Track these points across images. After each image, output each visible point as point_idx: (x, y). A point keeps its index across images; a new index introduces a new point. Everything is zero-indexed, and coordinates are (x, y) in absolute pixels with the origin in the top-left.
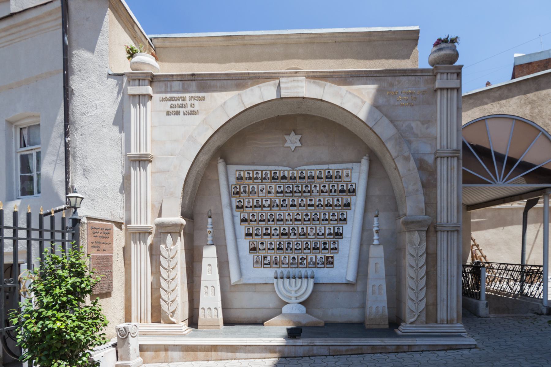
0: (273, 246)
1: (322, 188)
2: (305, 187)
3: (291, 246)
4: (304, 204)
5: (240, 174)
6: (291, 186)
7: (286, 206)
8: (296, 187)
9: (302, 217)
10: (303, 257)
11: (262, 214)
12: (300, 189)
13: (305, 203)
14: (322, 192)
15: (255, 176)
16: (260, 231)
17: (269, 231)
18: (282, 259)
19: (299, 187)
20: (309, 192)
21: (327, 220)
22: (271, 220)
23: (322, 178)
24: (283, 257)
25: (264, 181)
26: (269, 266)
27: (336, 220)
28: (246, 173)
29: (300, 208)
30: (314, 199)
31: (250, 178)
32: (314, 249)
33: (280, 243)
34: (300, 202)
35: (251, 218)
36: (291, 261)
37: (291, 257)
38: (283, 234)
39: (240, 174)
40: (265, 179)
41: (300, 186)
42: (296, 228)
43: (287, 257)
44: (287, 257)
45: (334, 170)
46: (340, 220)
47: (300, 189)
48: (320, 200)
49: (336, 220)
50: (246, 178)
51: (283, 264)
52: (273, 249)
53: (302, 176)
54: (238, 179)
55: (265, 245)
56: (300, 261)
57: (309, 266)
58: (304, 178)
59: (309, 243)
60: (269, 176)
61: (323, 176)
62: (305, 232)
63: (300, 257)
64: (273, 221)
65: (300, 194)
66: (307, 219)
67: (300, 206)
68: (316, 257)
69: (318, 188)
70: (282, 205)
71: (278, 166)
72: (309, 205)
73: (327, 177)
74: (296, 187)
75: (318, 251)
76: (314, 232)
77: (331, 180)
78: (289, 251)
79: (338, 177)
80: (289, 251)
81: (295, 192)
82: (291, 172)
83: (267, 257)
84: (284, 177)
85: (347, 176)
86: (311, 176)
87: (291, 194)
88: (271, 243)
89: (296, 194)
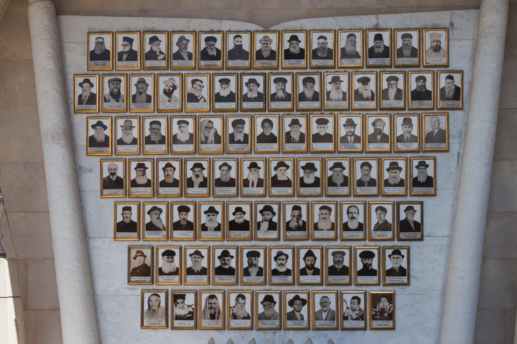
0: (204, 263)
1: (357, 86)
2: (305, 81)
3: (261, 262)
4: (302, 135)
5: (100, 43)
6: (260, 79)
7: (246, 141)
8: (276, 81)
9: (295, 172)
10: (297, 298)
11: (169, 165)
12: (289, 90)
13: (303, 130)
14: (359, 96)
15: (147, 48)
16: (163, 216)
17: (190, 217)
18: (233, 303)
19: (285, 81)
20: (316, 97)
21: (372, 183)
22: (197, 181)
23: (357, 56)
24: (233, 297)
25: (175, 63)
26: (192, 323)
27: (401, 183)
28: (120, 38)
29: (289, 147)
30: (331, 119)
31: (132, 56)
32: (332, 271)
33: (225, 254)
34: (287, 129)
35: (134, 175)
36: (261, 309)
37: (261, 297)
38: (234, 226)
39: (100, 43)
40: (178, 56)
41: (289, 78)
42: (275, 208)
43: (248, 296)
44: (248, 296)
45: (393, 32)
46: (416, 183)
47: (289, 90)
48: (350, 123)
49: (401, 183)
50: (121, 54)
51: (235, 317)
52: (204, 271)
53: (295, 50)
54: (93, 56)
55: (177, 258)
56: (289, 309)
57: (318, 323)
58: (301, 55)
59: (317, 253)
60: (191, 48)
61: (359, 48)
62: (304, 218)
63: (290, 297)
64: (203, 184)
65: (288, 105)
66: (309, 180)
67: (289, 139)
68: (339, 297)
69: (344, 87)
70: (232, 136)
71: (221, 18)
72: (317, 138)
73: (372, 53)
74: (276, 81)
75: (346, 279)
76: (332, 219)
77: (387, 61)
79: (407, 52)
80: (253, 278)
81: (274, 98)
82: (259, 37)
83: (183, 297)
84: (238, 53)
85: (437, 49)
86: (323, 48)
87: (261, 105)
88: (197, 253)
89: (274, 105)
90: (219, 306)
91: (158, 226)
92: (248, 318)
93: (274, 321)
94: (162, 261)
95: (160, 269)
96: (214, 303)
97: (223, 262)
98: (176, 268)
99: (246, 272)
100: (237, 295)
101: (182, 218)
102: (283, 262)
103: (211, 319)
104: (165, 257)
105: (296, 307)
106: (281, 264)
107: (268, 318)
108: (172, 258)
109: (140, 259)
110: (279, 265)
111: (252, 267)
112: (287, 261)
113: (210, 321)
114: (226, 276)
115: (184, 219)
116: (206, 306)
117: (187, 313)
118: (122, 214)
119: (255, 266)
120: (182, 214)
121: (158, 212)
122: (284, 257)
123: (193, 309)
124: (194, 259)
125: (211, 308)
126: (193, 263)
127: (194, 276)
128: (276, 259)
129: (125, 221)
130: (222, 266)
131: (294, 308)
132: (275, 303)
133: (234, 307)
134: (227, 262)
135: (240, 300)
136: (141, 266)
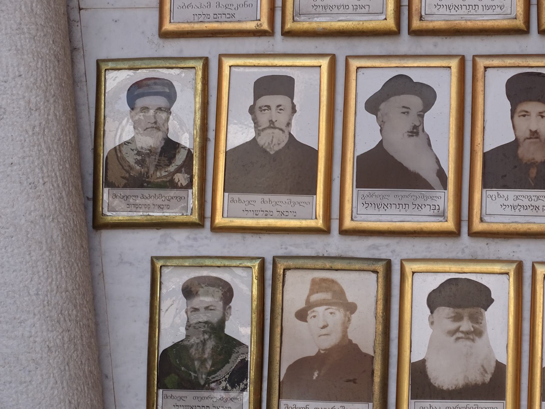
16: (440, 124)
55: (498, 320)
91: (412, 165)
94: (429, 331)
95: (419, 370)
98: (491, 368)
101: (524, 133)
104: (444, 312)
108: (476, 319)
109: (327, 316)
115: (535, 134)
118: (252, 110)
120: (526, 114)
121: (414, 102)
129: (263, 141)
136: (329, 352)
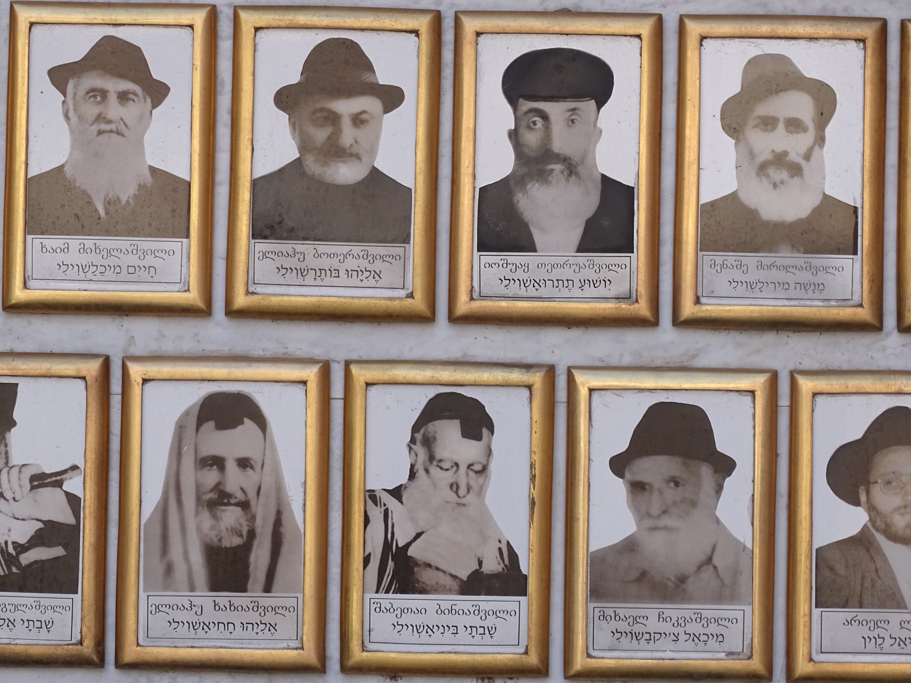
3: (617, 142)
18: (385, 457)
36: (608, 515)
37: (610, 426)
43: (514, 418)
44: (514, 418)
51: (402, 572)
56: (833, 520)
78: (558, 269)
80: (558, 269)
90: (279, 488)
92: (509, 581)
93: (710, 611)
96: (244, 463)
97: (320, 135)
99: (503, 227)
100: (421, 398)
102: (795, 145)
103: (216, 585)
105: (886, 500)
106: (780, 160)
107: (669, 588)
110: (763, 169)
111: (542, 176)
112: (820, 140)
113: (205, 599)
114: (341, 248)
116: (174, 485)
117: (22, 533)
119: (571, 168)
122: (800, 106)
123: (73, 501)
124: (91, 110)
125: (219, 499)
126: (78, 140)
127: (89, 242)
128: (735, 118)
130: (313, 166)
131: (871, 509)
132: (725, 466)
133: (396, 493)
134: (348, 135)
135: (449, 436)
